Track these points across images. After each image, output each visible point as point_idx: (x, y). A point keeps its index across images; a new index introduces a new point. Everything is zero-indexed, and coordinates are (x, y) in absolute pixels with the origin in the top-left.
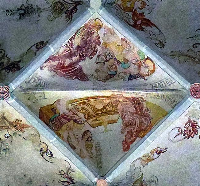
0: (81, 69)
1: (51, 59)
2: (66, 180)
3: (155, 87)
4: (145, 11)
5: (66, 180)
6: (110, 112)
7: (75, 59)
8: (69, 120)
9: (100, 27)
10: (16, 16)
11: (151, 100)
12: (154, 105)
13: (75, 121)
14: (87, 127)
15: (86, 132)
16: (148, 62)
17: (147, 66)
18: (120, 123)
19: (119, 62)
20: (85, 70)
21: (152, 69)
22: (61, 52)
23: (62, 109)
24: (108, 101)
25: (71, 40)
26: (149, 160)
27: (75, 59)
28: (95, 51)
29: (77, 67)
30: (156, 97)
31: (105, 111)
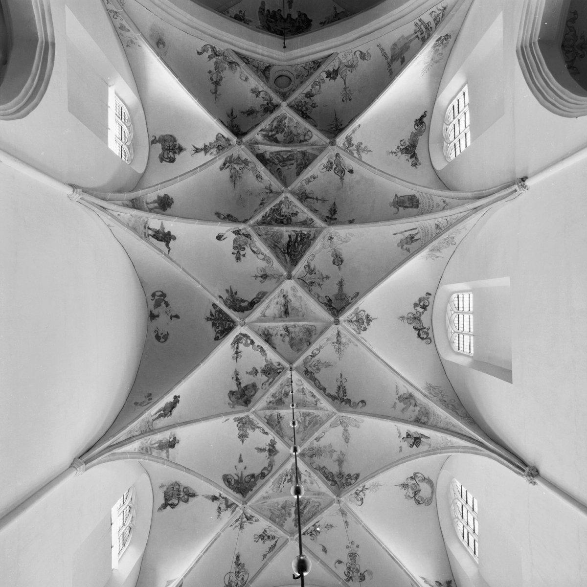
0: (276, 138)
1: (262, 130)
2: (268, 191)
3: (313, 145)
4: (307, 112)
5: (268, 191)
6: (291, 160)
7: (274, 132)
8: (271, 162)
10: (246, 115)
11: (310, 151)
12: (312, 153)
13: (273, 163)
14: (279, 167)
15: (279, 169)
16: (309, 133)
17: (308, 135)
18: (295, 165)
19: (295, 135)
20: (278, 139)
21: (311, 136)
22: (267, 127)
23: (267, 156)
24: (289, 154)
25: (272, 122)
26: (309, 181)
27: (274, 132)
28: (283, 131)
30: (313, 149)
31: (288, 159)
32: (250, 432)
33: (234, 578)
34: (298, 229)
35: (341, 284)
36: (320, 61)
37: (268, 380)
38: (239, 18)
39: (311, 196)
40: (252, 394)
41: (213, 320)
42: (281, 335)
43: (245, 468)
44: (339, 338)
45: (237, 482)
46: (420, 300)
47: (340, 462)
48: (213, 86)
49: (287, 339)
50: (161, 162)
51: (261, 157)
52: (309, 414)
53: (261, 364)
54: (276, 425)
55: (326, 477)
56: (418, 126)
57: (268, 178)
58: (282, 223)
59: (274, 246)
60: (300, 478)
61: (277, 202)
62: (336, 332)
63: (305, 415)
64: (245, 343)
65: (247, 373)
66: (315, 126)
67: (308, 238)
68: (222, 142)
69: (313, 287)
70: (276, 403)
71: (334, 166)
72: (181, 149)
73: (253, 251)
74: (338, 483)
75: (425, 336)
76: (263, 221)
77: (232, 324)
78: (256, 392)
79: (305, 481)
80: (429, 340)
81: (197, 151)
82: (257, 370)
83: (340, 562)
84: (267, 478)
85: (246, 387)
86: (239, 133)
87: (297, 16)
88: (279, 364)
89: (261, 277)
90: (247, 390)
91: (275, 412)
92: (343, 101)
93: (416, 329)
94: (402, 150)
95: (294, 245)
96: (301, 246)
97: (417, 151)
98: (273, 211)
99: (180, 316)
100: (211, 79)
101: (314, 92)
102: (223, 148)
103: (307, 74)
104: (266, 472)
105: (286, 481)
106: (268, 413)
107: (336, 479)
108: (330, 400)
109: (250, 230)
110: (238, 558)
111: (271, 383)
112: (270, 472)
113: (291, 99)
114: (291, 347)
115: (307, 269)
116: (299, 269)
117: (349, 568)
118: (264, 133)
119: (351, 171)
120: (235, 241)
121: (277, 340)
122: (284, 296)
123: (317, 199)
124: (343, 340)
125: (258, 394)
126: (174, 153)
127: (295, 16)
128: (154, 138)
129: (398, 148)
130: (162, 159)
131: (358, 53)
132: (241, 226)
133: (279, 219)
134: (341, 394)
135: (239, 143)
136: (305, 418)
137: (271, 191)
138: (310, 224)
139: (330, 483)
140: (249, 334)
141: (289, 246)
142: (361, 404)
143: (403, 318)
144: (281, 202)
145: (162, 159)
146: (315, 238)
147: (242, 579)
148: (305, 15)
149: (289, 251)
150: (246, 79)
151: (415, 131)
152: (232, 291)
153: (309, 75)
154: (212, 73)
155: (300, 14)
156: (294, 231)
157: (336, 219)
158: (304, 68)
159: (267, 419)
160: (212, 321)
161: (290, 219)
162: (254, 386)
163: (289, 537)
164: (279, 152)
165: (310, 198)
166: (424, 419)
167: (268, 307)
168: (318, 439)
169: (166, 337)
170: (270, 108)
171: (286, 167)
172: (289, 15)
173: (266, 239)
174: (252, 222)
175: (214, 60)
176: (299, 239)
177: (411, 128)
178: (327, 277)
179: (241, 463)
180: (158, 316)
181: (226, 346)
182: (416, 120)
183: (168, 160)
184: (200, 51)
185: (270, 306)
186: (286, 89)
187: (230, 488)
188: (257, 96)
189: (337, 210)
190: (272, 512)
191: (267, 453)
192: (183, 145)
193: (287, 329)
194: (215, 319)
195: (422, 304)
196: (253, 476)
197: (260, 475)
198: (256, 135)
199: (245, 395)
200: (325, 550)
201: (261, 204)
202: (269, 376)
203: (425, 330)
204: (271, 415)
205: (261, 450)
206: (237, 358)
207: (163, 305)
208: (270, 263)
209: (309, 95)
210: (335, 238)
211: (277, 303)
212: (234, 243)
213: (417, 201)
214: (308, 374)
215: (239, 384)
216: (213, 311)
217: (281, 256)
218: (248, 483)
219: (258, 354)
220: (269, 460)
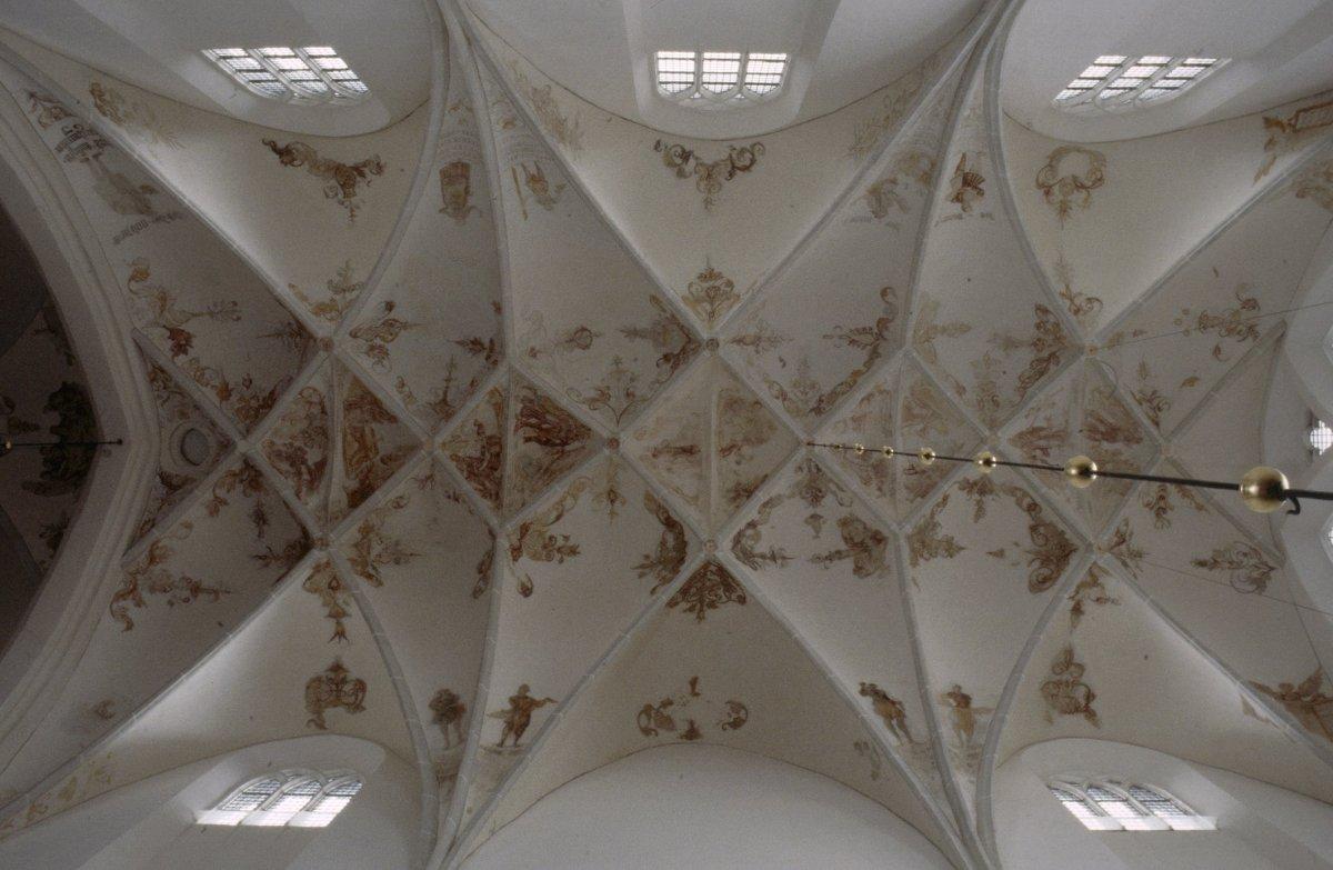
0: (316, 464)
2: (429, 483)
9: (272, 443)
10: (265, 528)
13: (369, 471)
16: (305, 393)
18: (373, 425)
19: (311, 424)
20: (318, 459)
21: (311, 391)
22: (293, 484)
23: (353, 484)
24: (349, 437)
26: (410, 395)
29: (313, 467)
31: (361, 439)
32: (941, 534)
33: (1242, 572)
34: (512, 424)
35: (633, 333)
36: (150, 368)
37: (834, 493)
38: (56, 538)
39: (441, 393)
40: (860, 527)
41: (702, 606)
42: (738, 463)
43: (1017, 544)
44: (748, 340)
45: (1046, 561)
46: (670, 164)
47: (1010, 344)
48: (201, 596)
49: (747, 450)
50: (364, 709)
51: (358, 496)
52: (908, 409)
53: (799, 508)
54: (929, 477)
55: (1042, 374)
56: (294, 160)
57: (401, 484)
58: (498, 455)
59: (548, 474)
60: (1042, 429)
61: (452, 466)
62: (735, 345)
63: (910, 416)
64: (753, 539)
65: (817, 537)
66: (290, 380)
67: (531, 401)
68: (323, 580)
69: (638, 393)
70: (882, 476)
71: (378, 341)
72: (337, 668)
73: (558, 518)
74: (1053, 349)
75: (748, 155)
76: (494, 497)
77: (713, 568)
78: (858, 520)
79: (1048, 419)
80: (757, 147)
81: (340, 634)
82: (812, 517)
83: (1217, 351)
84: (1038, 500)
85: (845, 539)
86: (302, 546)
87: (57, 413)
88: (800, 468)
89: (612, 502)
90: (852, 539)
91: (902, 478)
92: (239, 319)
93: (731, 175)
94: (346, 196)
95: (547, 430)
96: (549, 417)
97: (350, 161)
98: (472, 475)
99: (693, 675)
100: (187, 600)
101: (217, 382)
102: (335, 578)
103: (178, 397)
104: (1027, 501)
105: (1046, 459)
106: (902, 494)
107: (1045, 354)
108: (878, 361)
109: (511, 527)
110: (1202, 564)
111: (838, 487)
112: (1026, 494)
113: (232, 431)
114: (761, 441)
115: (600, 404)
116: (599, 422)
117: (1230, 332)
118: (304, 489)
119: (390, 306)
120: (535, 557)
121: (747, 473)
122: (654, 456)
123: (448, 380)
124: (752, 331)
125: (865, 517)
126: (344, 681)
127: (54, 419)
128: (312, 724)
129: (343, 204)
130: (357, 707)
131: (134, 286)
132: (504, 543)
133: (489, 462)
134: (868, 339)
135: (325, 544)
136: (915, 417)
137: (430, 477)
138: (500, 395)
139: (1053, 368)
140: (735, 532)
141: (547, 443)
142: (890, 298)
143: (708, 203)
144: (455, 458)
145: (357, 707)
146: (531, 388)
147: (1245, 555)
148: (54, 396)
149: (558, 441)
150: (189, 526)
151: (306, 166)
152: (642, 566)
153: (181, 392)
154: (174, 600)
155: (52, 407)
156: (516, 431)
157: (492, 341)
158: (164, 402)
159: (916, 497)
160: (705, 608)
161: (490, 438)
162: (844, 523)
163: (1163, 457)
164: (345, 459)
165: (445, 393)
166: (925, 164)
167: (677, 490)
168: (961, 390)
169: (737, 707)
170: (251, 477)
171: (379, 444)
172: (53, 430)
173: (533, 491)
174: (494, 522)
175: (145, 595)
176: (533, 421)
177: (300, 174)
178: (617, 362)
179: (1007, 553)
180: (692, 723)
181: (758, 582)
182: (282, 162)
183: (360, 695)
184: (125, 626)
185: (677, 485)
186: (212, 441)
187: (1057, 578)
188: (226, 503)
189: (472, 339)
190: (1110, 491)
191: (988, 499)
192: (329, 661)
193: (725, 451)
194: (701, 601)
195: (678, 161)
196: (1033, 529)
197: (1033, 513)
198: (308, 507)
199: (862, 543)
200: (1191, 381)
201: (457, 500)
202: (823, 489)
203: (734, 156)
204: (907, 488)
205: (980, 511)
206: (784, 558)
207: (668, 711)
208: (583, 483)
209: (225, 392)
210: (532, 344)
211: (669, 470)
212: (538, 559)
213: (455, 165)
214: (822, 407)
215: (838, 555)
216: (684, 605)
217: (568, 460)
218: (1047, 540)
219: (777, 512)
220: (1001, 494)
